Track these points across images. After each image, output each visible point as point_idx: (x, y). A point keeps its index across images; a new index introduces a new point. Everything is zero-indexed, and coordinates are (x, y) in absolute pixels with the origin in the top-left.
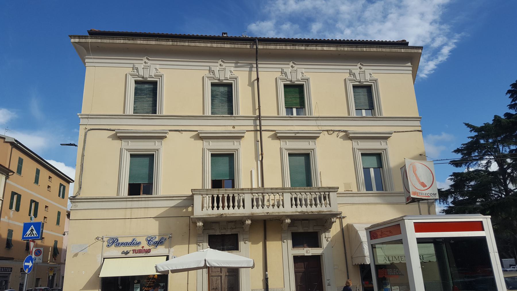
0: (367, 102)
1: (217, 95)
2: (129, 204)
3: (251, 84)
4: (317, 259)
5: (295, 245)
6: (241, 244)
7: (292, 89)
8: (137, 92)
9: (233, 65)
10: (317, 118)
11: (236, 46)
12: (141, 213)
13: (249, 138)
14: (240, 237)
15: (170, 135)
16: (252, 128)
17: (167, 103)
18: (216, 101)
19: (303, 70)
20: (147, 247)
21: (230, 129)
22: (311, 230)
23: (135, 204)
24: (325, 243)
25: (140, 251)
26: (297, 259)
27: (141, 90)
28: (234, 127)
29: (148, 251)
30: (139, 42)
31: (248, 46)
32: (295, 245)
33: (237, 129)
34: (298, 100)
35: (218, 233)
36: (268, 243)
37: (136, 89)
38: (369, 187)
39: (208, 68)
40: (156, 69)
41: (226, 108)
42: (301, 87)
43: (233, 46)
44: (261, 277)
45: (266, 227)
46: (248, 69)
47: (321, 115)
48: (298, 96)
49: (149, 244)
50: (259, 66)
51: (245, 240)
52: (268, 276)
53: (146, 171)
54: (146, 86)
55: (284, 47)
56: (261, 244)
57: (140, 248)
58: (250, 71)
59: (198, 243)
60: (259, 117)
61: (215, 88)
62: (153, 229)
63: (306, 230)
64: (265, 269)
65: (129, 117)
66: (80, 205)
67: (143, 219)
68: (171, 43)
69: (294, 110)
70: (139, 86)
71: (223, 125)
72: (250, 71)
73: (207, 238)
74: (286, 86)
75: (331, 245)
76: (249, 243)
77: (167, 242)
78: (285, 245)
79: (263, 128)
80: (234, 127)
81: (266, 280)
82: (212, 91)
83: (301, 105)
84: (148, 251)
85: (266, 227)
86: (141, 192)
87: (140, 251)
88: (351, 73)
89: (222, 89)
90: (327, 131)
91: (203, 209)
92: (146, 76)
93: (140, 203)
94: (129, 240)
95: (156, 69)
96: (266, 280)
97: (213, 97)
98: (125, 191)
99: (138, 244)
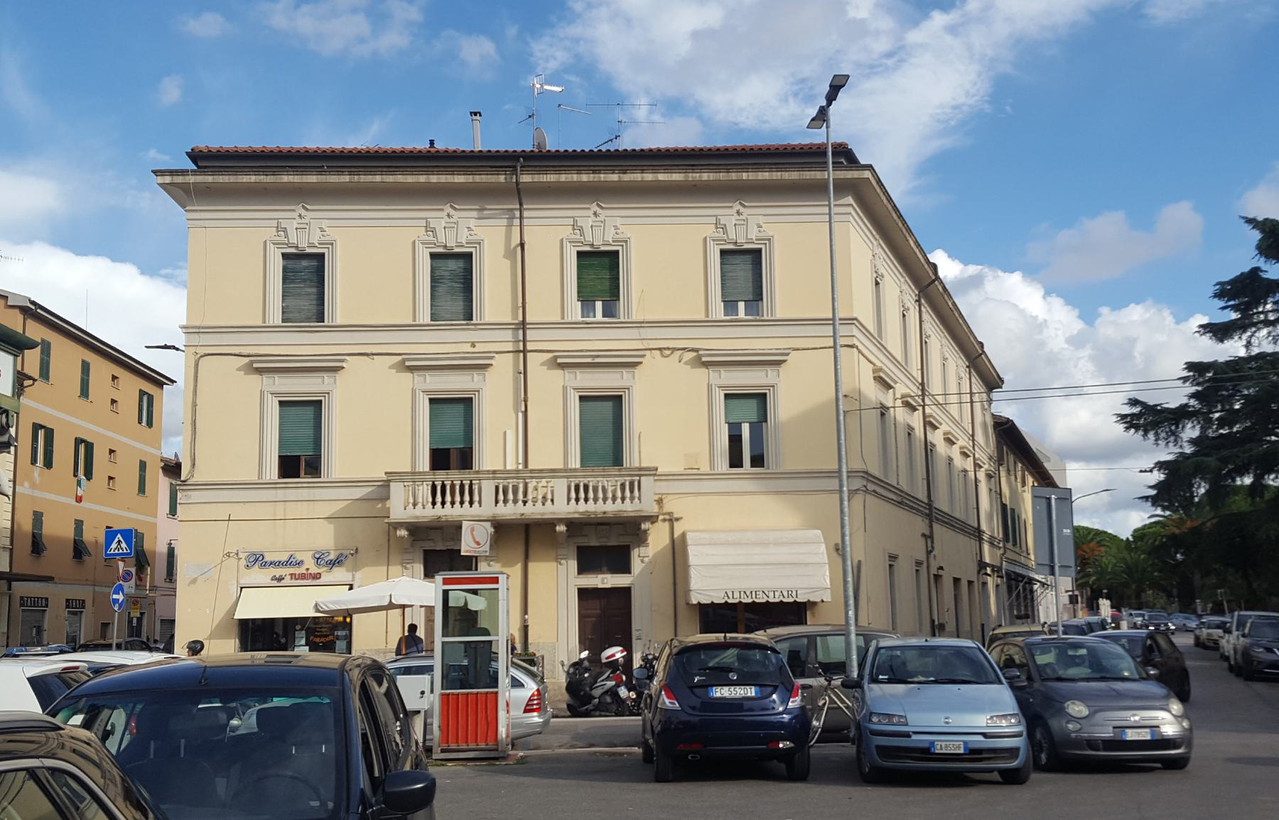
1: (442, 277)
2: (280, 494)
3: (510, 254)
4: (625, 592)
5: (582, 570)
7: (595, 261)
9: (475, 214)
10: (641, 324)
11: (478, 178)
13: (504, 367)
15: (351, 363)
16: (510, 347)
17: (343, 299)
18: (441, 289)
20: (314, 570)
23: (292, 494)
24: (637, 565)
25: (303, 577)
26: (584, 593)
27: (294, 271)
28: (473, 345)
29: (317, 576)
31: (502, 178)
32: (582, 570)
33: (479, 348)
34: (607, 283)
36: (531, 565)
38: (736, 461)
41: (459, 305)
43: (470, 179)
46: (505, 222)
47: (648, 318)
48: (606, 275)
50: (526, 214)
52: (530, 623)
54: (305, 263)
55: (575, 177)
57: (302, 570)
58: (510, 226)
59: (404, 564)
60: (523, 325)
61: (440, 263)
62: (325, 538)
63: (605, 543)
65: (273, 329)
67: (307, 519)
70: (291, 264)
71: (452, 341)
72: (510, 226)
74: (580, 254)
75: (650, 570)
77: (350, 561)
78: (562, 569)
79: (530, 346)
80: (473, 345)
84: (317, 576)
87: (303, 577)
89: (453, 265)
90: (660, 349)
93: (300, 490)
94: (284, 558)
97: (435, 281)
99: (300, 563)
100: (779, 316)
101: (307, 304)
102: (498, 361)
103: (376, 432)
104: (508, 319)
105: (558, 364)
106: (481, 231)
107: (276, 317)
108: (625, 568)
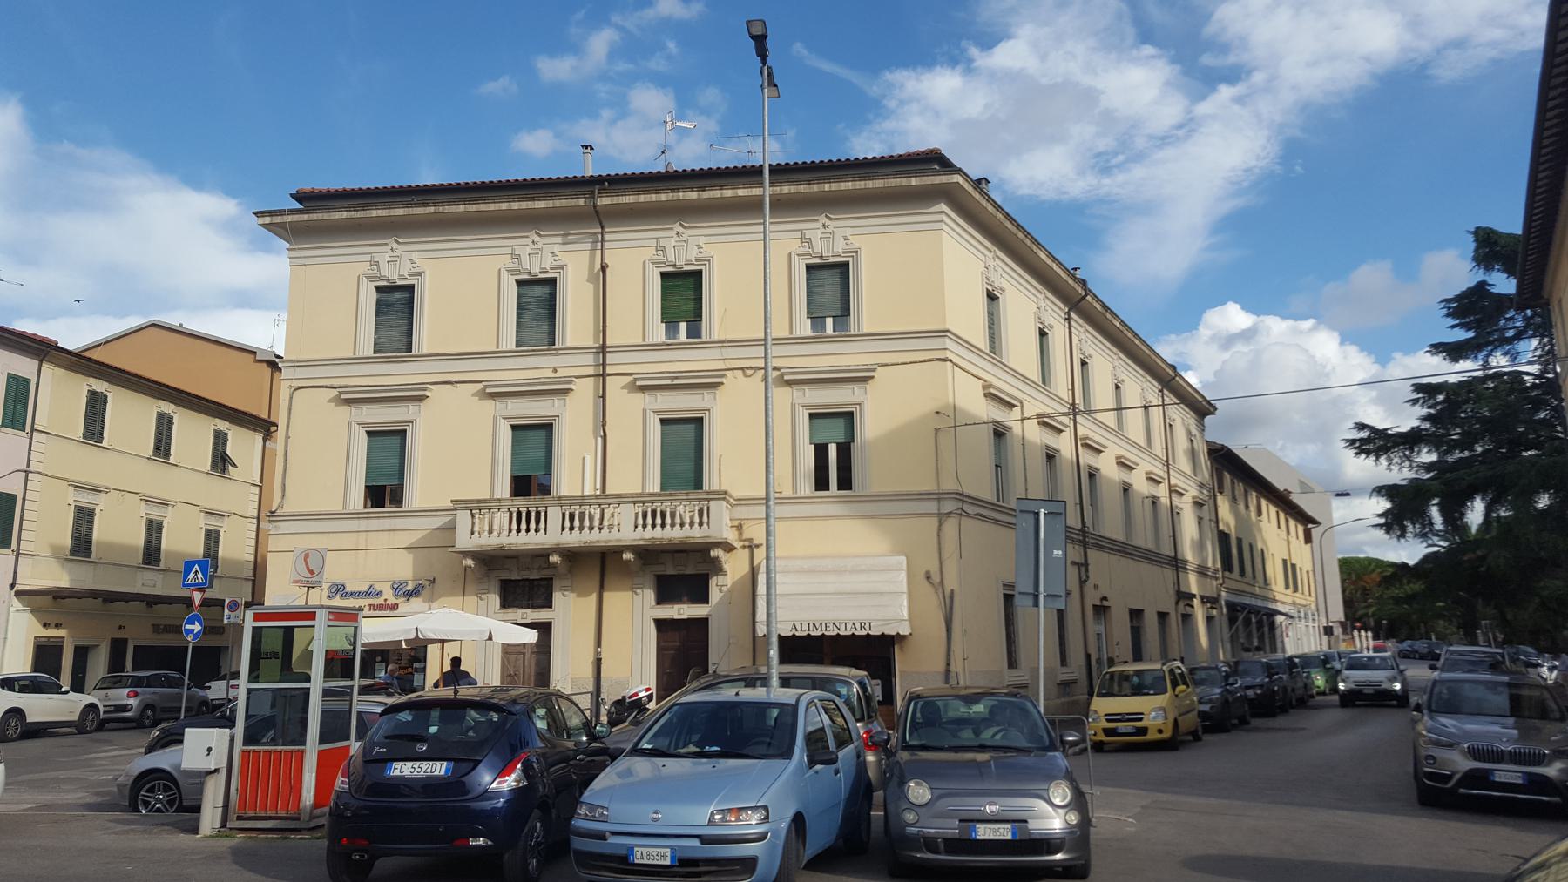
0: (838, 300)
1: (529, 303)
2: (363, 524)
3: (592, 278)
4: (703, 623)
5: (661, 599)
6: (557, 597)
7: (679, 282)
8: (381, 308)
9: (559, 239)
10: (722, 344)
11: (558, 203)
12: (383, 540)
13: (584, 391)
14: (556, 583)
15: (434, 393)
16: (591, 371)
17: (430, 331)
18: (527, 317)
19: (848, 232)
20: (392, 600)
21: (550, 373)
22: (690, 571)
23: (374, 524)
24: (715, 595)
25: (380, 607)
26: (661, 624)
27: (388, 304)
29: (394, 607)
30: (374, 213)
31: (581, 202)
32: (661, 599)
35: (515, 577)
36: (606, 595)
37: (379, 302)
38: (821, 483)
39: (509, 250)
40: (699, 247)
41: (543, 333)
42: (843, 267)
43: (550, 204)
44: (591, 658)
45: (600, 566)
46: (588, 246)
47: (730, 337)
49: (396, 595)
50: (608, 237)
51: (563, 589)
52: (603, 656)
53: (396, 461)
54: (397, 295)
55: (654, 197)
56: (594, 597)
57: (380, 601)
59: (479, 594)
60: (603, 349)
61: (526, 290)
62: (404, 568)
63: (681, 572)
64: (599, 643)
65: (365, 360)
66: (285, 527)
68: (431, 210)
69: (829, 321)
70: (385, 296)
71: (536, 368)
72: (593, 250)
73: (496, 586)
75: (728, 600)
76: (572, 596)
77: (425, 593)
78: (638, 599)
79: (609, 370)
81: (598, 662)
82: (519, 297)
83: (844, 312)
84: (394, 607)
85: (600, 566)
86: (387, 502)
87: (380, 607)
88: (804, 240)
89: (539, 291)
91: (500, 534)
92: (535, 269)
94: (364, 588)
95: (699, 247)
96: (598, 662)
97: (521, 308)
98: (357, 499)
99: (379, 594)
100: (866, 330)
101: (397, 336)
102: (577, 385)
103: (458, 458)
104: (591, 343)
105: (641, 387)
106: (563, 256)
107: (367, 349)
108: (704, 599)
